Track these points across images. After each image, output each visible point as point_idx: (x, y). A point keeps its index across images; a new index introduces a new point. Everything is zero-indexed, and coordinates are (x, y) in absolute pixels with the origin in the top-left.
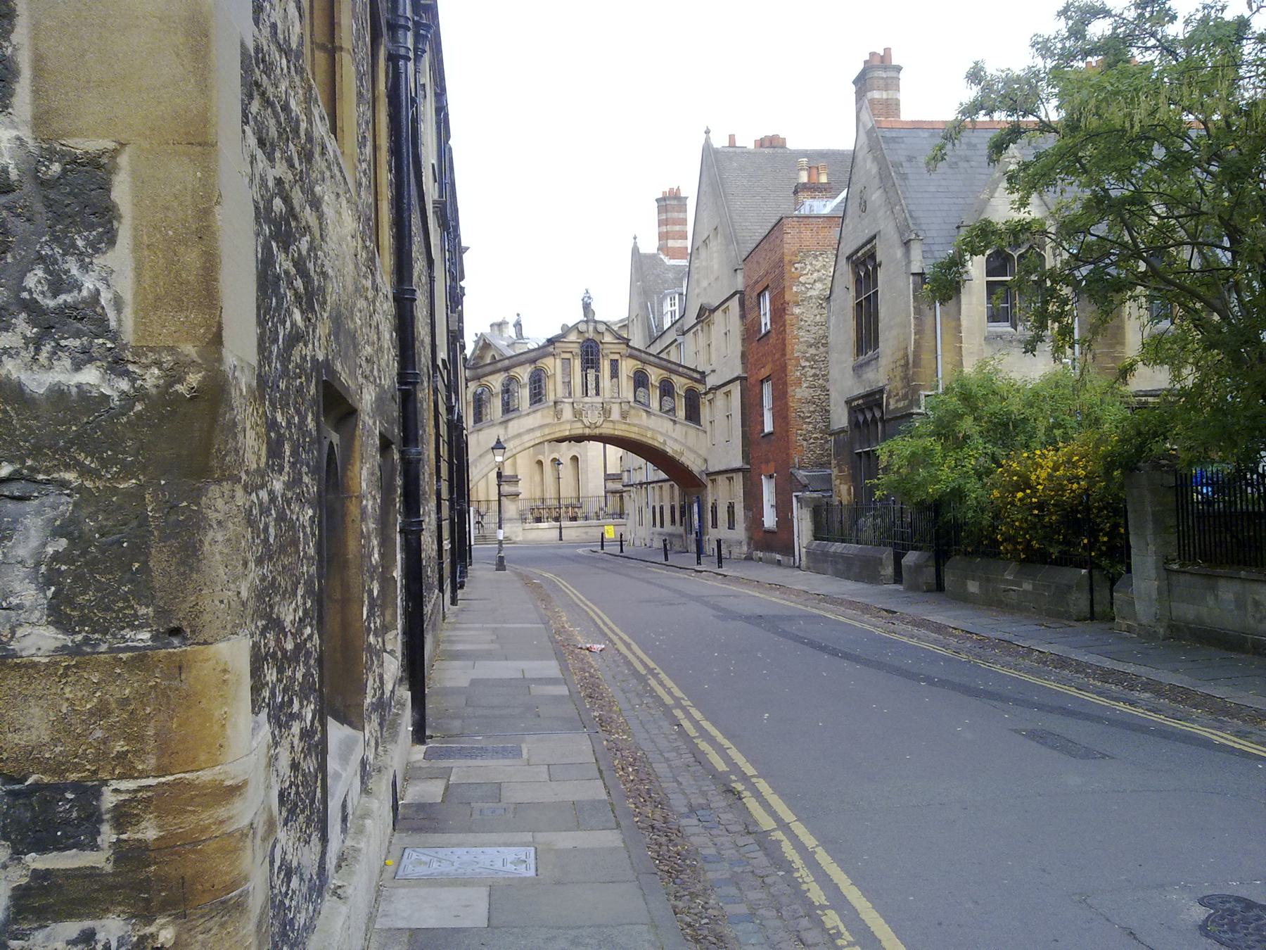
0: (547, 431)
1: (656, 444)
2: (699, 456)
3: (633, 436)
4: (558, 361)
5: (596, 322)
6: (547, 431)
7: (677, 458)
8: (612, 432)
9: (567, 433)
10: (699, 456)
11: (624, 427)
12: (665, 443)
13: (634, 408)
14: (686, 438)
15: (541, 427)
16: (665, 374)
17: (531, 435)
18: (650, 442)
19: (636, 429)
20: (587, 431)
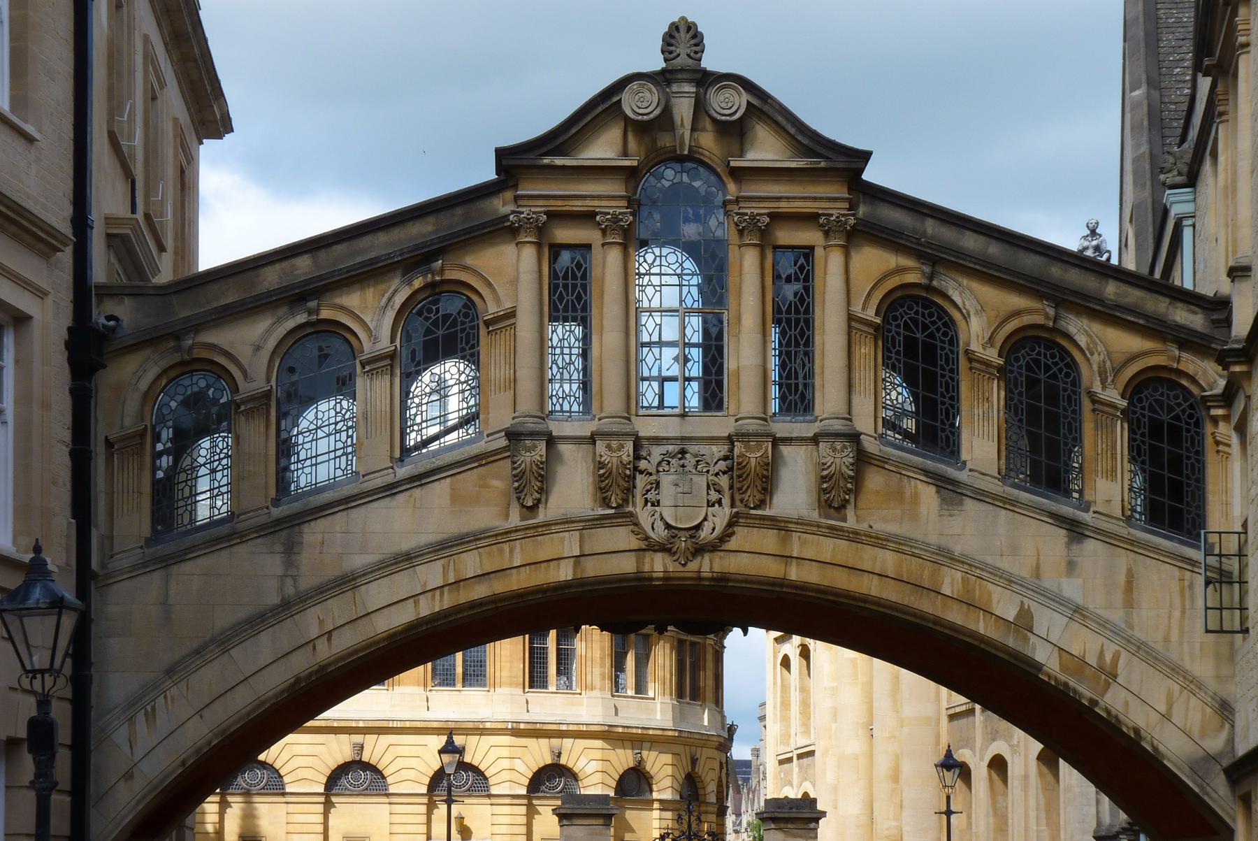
0: (471, 563)
1: (982, 626)
2: (1192, 684)
3: (871, 587)
4: (529, 253)
5: (706, 80)
6: (471, 563)
7: (1085, 691)
8: (772, 569)
9: (565, 573)
10: (1192, 684)
11: (829, 548)
12: (1024, 623)
13: (881, 462)
14: (1130, 601)
15: (446, 547)
16: (1033, 311)
17: (402, 583)
18: (955, 616)
19: (887, 560)
20: (658, 565)
